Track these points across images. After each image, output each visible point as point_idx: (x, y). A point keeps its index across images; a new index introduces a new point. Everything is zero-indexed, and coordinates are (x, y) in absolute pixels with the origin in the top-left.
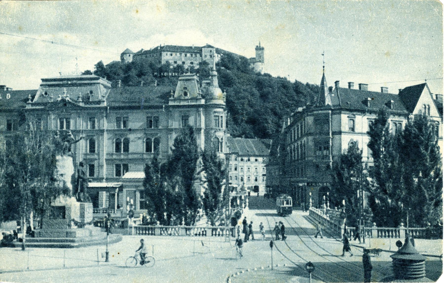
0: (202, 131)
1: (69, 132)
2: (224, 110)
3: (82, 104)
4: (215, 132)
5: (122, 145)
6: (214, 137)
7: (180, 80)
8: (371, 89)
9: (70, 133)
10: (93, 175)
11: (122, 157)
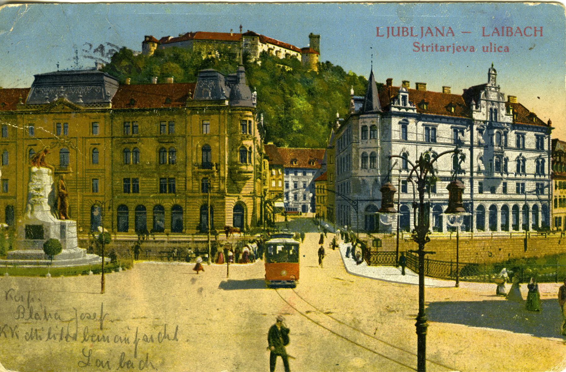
4: (242, 139)
8: (429, 88)
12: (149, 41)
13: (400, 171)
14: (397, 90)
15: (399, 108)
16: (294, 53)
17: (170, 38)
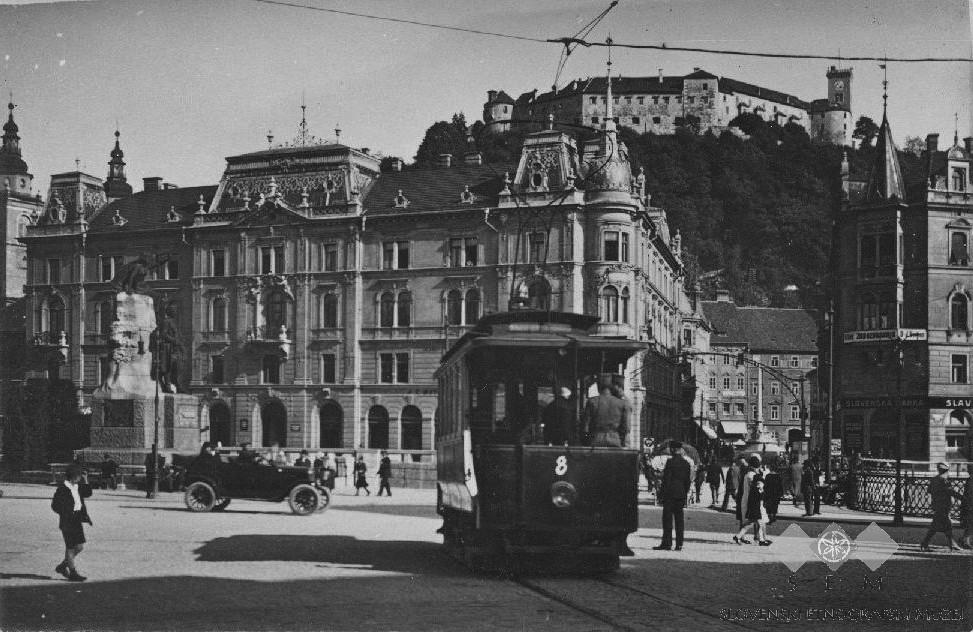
0: (577, 272)
1: (281, 280)
2: (634, 219)
4: (608, 272)
6: (606, 285)
9: (285, 282)
10: (333, 381)
11: (396, 337)
12: (498, 102)
13: (949, 334)
14: (944, 157)
15: (948, 196)
16: (796, 112)
17: (537, 95)
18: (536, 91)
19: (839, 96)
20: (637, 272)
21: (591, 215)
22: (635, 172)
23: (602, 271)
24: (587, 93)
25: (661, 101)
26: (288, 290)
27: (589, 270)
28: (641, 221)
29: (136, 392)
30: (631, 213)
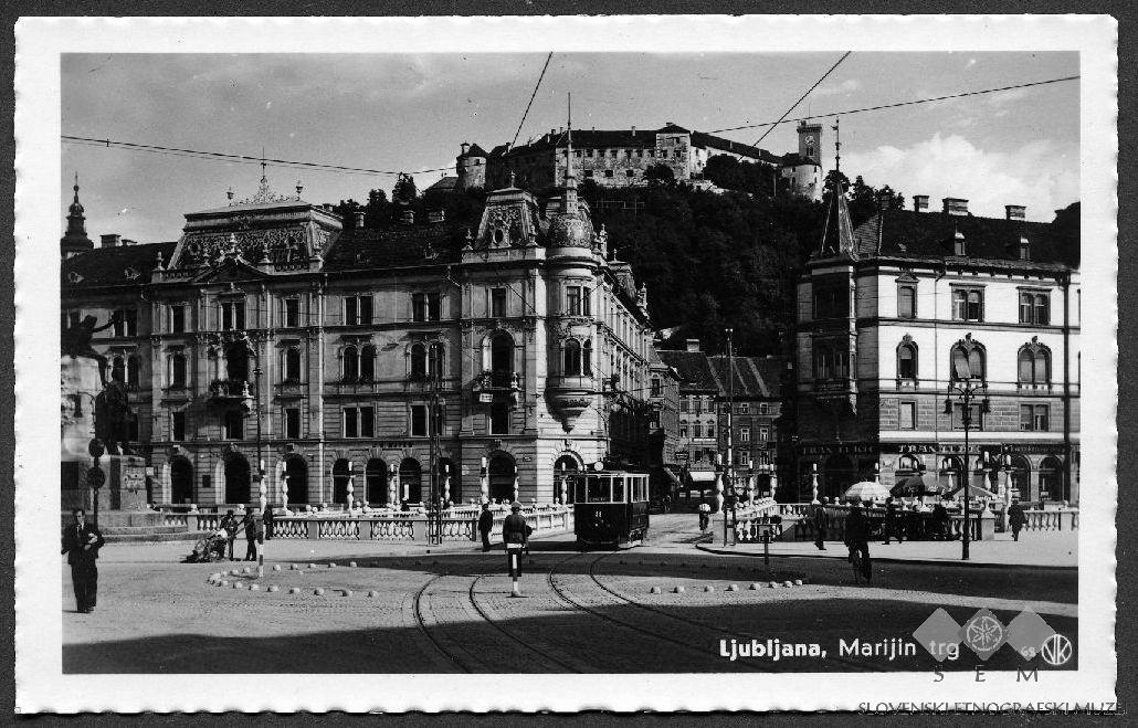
0: (540, 327)
3: (269, 271)
4: (570, 325)
5: (358, 364)
7: (490, 204)
18: (508, 144)
19: (810, 151)
20: (599, 325)
21: (553, 270)
22: (597, 229)
23: (564, 325)
24: (559, 147)
25: (635, 155)
26: (250, 346)
27: (552, 320)
28: (603, 277)
29: (80, 454)
30: (592, 268)
